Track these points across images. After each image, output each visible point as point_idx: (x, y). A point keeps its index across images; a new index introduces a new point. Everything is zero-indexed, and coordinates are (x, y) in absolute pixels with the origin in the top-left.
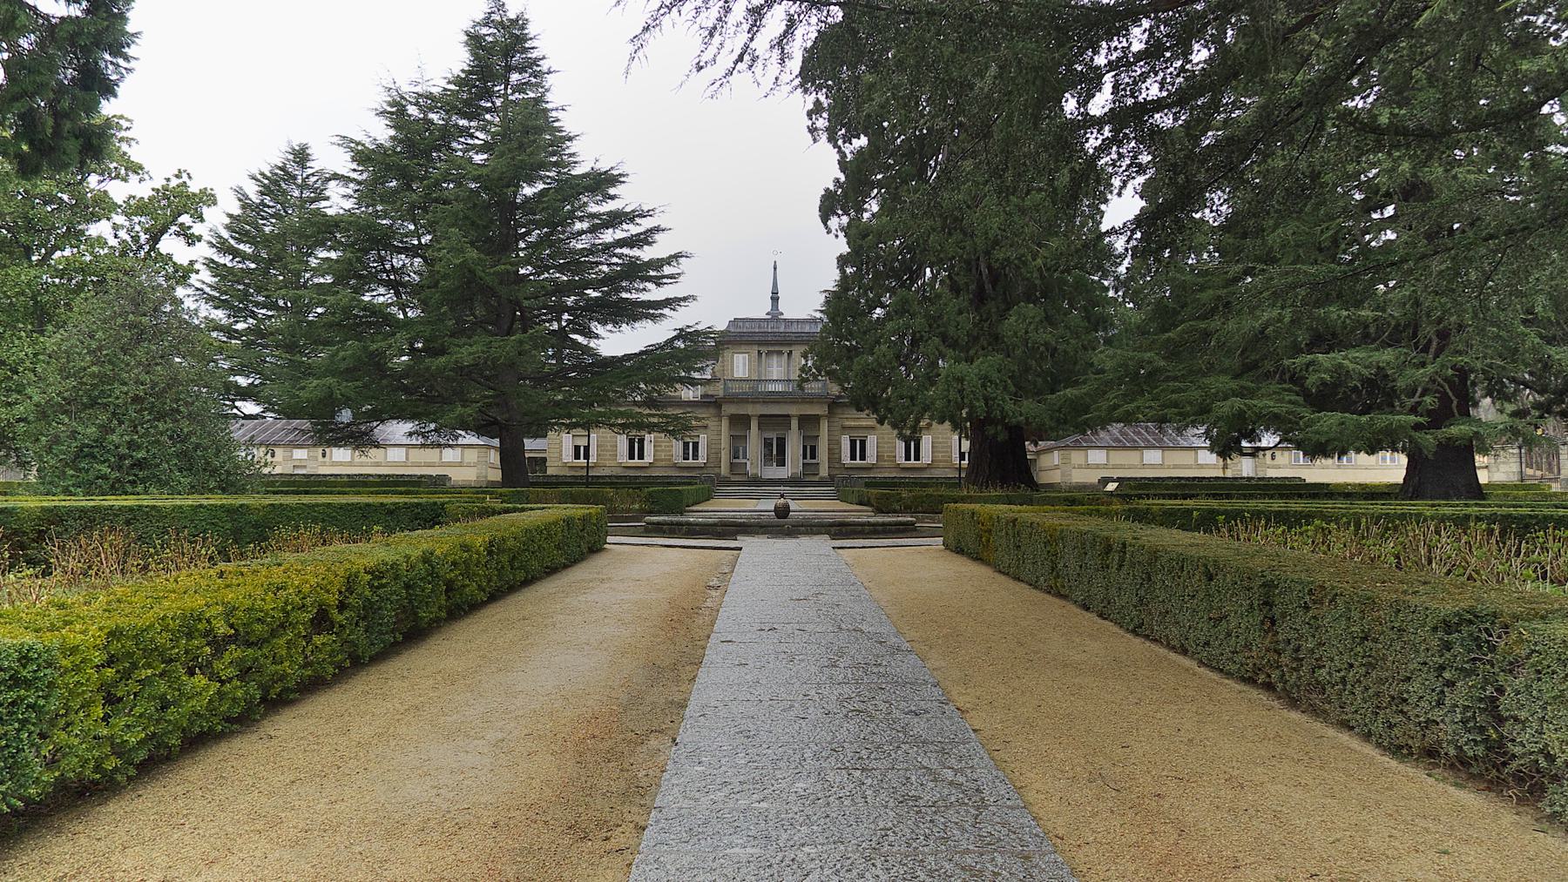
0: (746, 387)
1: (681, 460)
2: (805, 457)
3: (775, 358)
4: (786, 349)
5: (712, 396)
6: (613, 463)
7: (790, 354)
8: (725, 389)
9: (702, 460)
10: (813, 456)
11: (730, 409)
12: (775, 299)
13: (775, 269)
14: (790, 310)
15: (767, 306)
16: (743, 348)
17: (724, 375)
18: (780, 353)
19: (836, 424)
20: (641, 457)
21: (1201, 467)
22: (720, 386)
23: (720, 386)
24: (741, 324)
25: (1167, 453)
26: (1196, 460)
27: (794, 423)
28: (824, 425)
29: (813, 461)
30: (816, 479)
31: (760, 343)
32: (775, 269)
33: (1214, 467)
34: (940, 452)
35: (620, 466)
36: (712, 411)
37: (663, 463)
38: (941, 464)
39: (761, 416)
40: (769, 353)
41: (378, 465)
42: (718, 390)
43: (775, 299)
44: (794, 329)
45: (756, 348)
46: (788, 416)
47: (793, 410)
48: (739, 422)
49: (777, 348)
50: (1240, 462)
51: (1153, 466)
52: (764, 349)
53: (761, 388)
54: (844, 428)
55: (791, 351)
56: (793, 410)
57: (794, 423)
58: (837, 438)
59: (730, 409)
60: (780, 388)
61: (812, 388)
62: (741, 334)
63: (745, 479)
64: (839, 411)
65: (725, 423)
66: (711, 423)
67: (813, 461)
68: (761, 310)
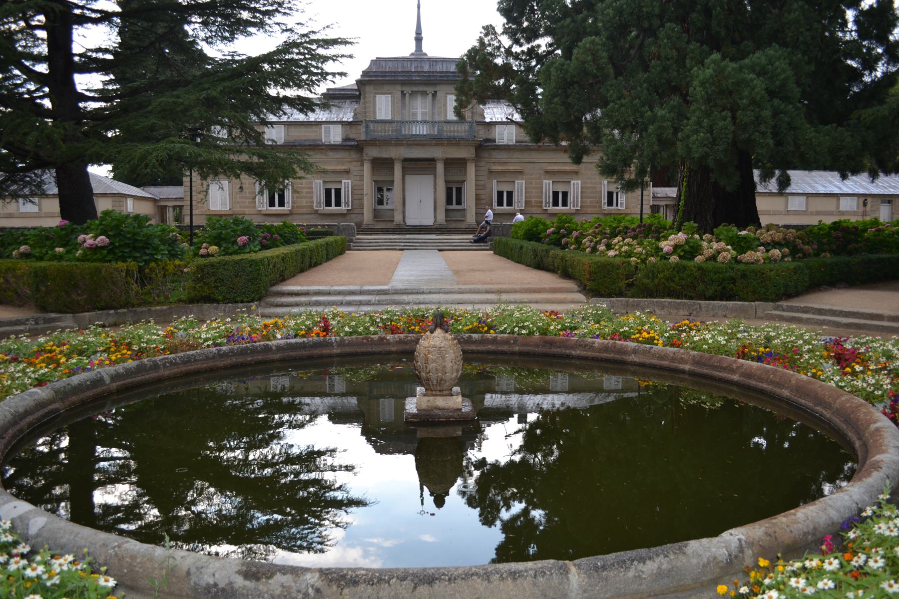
0: (389, 131)
1: (323, 208)
2: (449, 201)
3: (419, 100)
4: (430, 90)
5: (354, 140)
6: (252, 211)
7: (434, 95)
8: (367, 133)
9: (343, 208)
10: (459, 202)
11: (373, 152)
12: (419, 39)
13: (419, 7)
14: (432, 49)
15: (412, 49)
16: (386, 88)
17: (366, 116)
18: (424, 94)
19: (482, 169)
20: (282, 204)
21: (843, 213)
22: (362, 129)
23: (362, 129)
24: (383, 64)
25: (811, 199)
26: (838, 207)
27: (440, 167)
28: (471, 169)
29: (459, 207)
30: (463, 226)
31: (403, 83)
32: (419, 7)
33: (854, 213)
34: (588, 198)
35: (259, 213)
36: (354, 155)
37: (304, 211)
38: (589, 210)
39: (405, 160)
40: (413, 94)
41: (10, 216)
42: (360, 134)
43: (419, 39)
44: (439, 68)
45: (399, 88)
46: (433, 160)
47: (437, 153)
48: (382, 165)
49: (421, 88)
50: (878, 209)
51: (796, 213)
52: (408, 89)
53: (405, 131)
54: (491, 172)
55: (436, 92)
56: (437, 153)
57: (440, 167)
58: (483, 183)
59: (373, 152)
60: (422, 130)
61: (458, 132)
62: (384, 74)
63: (389, 226)
64: (486, 154)
65: (367, 167)
66: (353, 167)
67: (459, 207)
68: (406, 49)
